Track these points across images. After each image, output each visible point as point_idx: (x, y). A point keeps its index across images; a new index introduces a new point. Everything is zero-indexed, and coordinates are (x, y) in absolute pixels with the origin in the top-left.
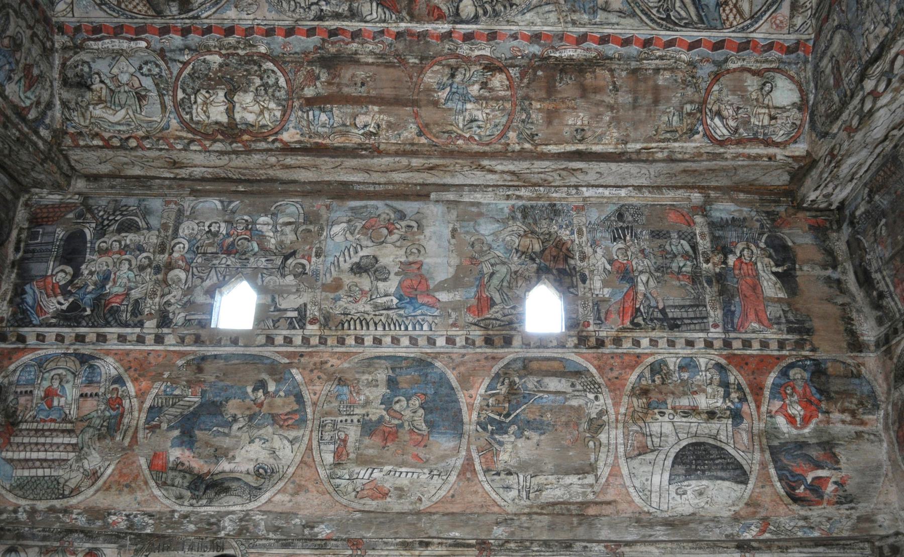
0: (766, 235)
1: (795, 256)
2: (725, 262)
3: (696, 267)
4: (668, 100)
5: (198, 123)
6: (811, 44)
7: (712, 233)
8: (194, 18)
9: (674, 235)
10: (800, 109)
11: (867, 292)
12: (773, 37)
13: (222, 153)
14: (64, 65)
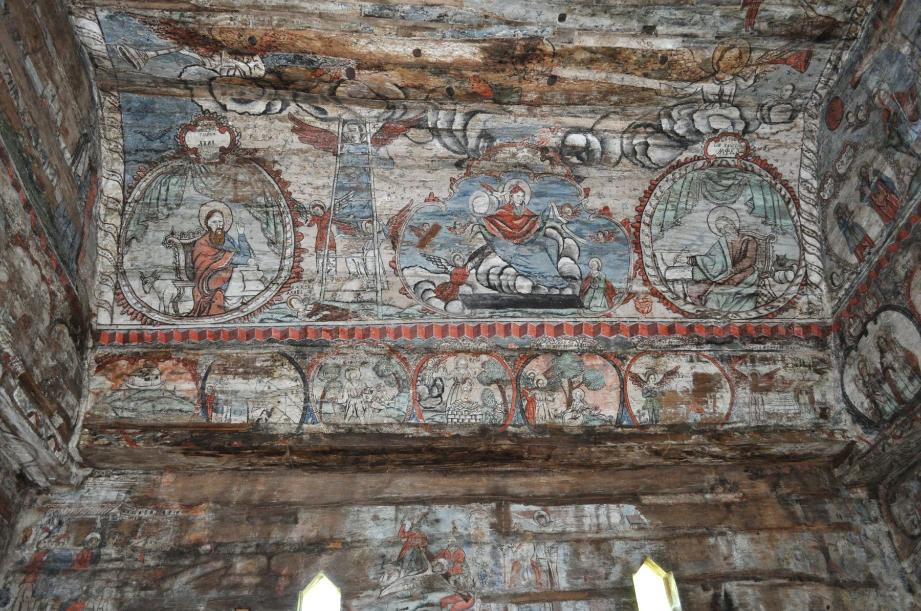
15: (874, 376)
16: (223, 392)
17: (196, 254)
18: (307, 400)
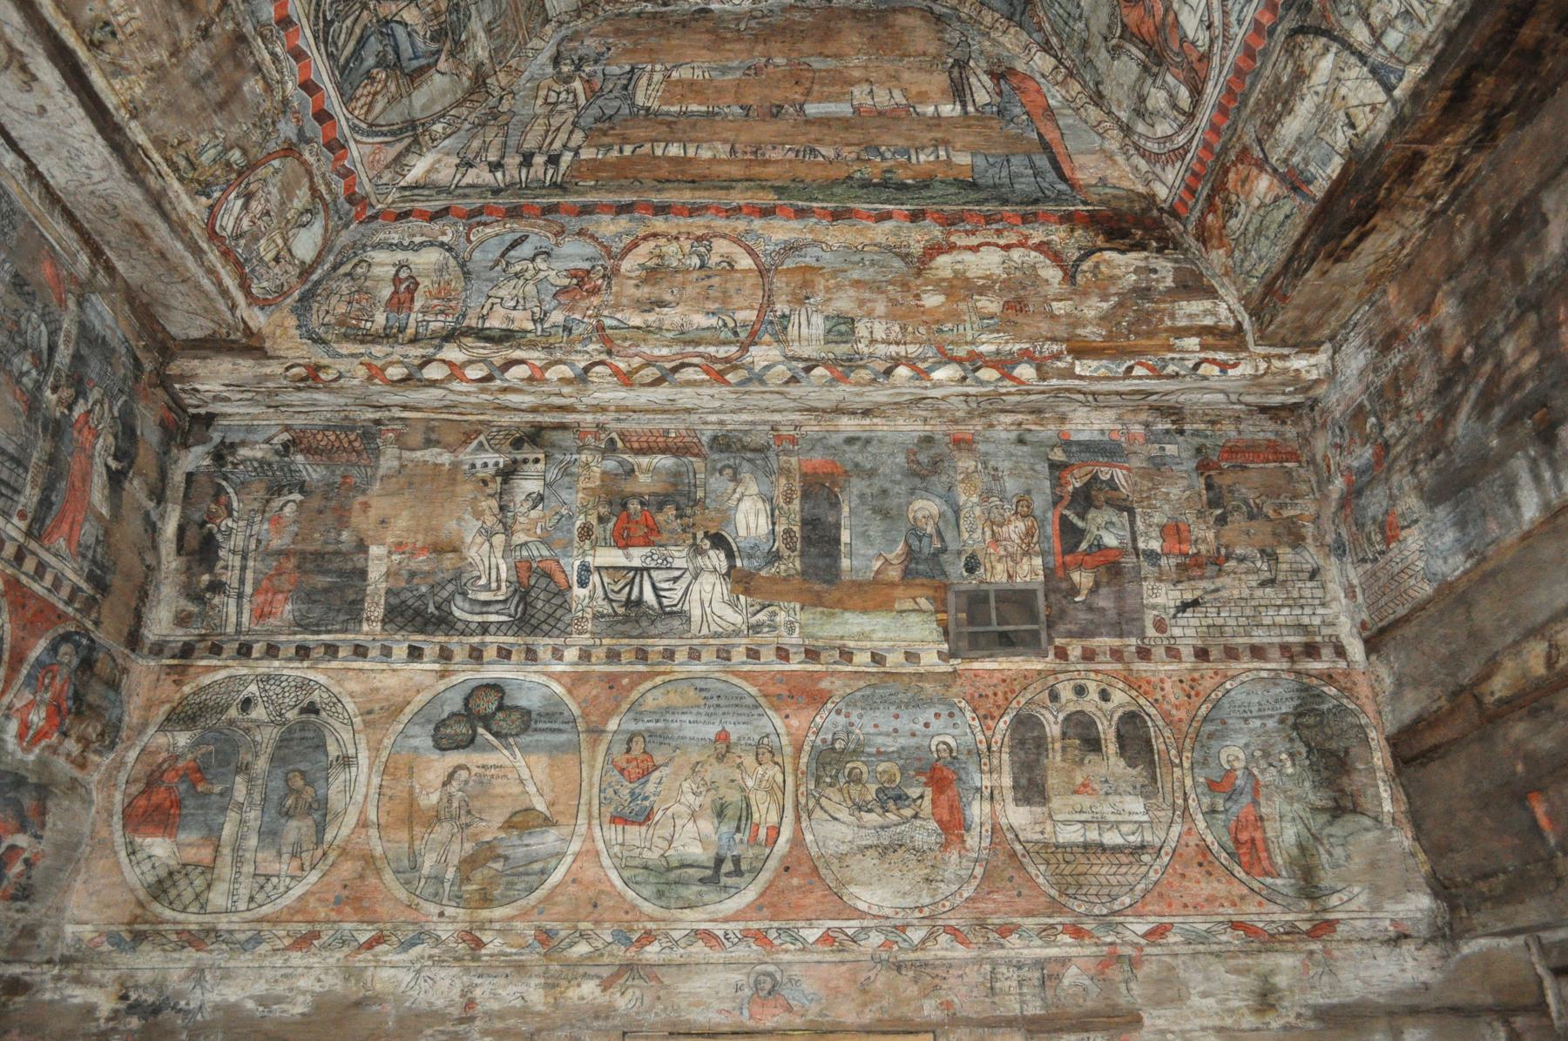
0: (124, 398)
1: (136, 455)
2: (70, 408)
3: (39, 386)
4: (232, 121)
6: (370, 212)
7: (77, 343)
9: (39, 305)
10: (301, 274)
11: (189, 568)
12: (359, 166)
16: (1292, 153)
17: (1135, 30)
18: (1363, 58)
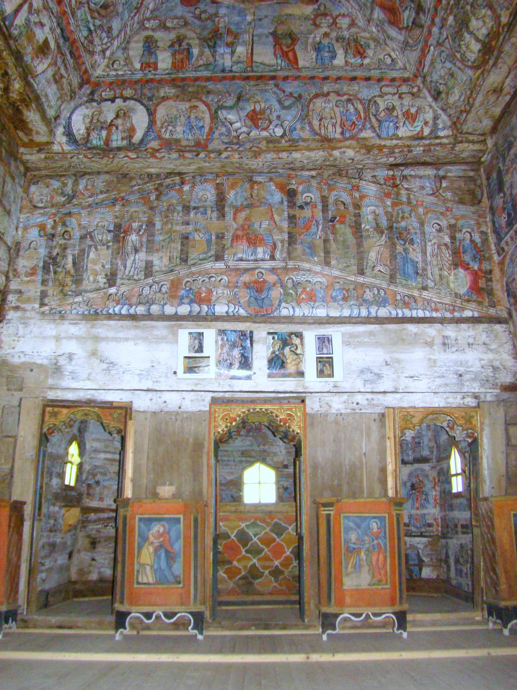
5: (475, 60)
8: (429, 11)
13: (495, 64)
14: (429, 92)
15: (101, 123)
